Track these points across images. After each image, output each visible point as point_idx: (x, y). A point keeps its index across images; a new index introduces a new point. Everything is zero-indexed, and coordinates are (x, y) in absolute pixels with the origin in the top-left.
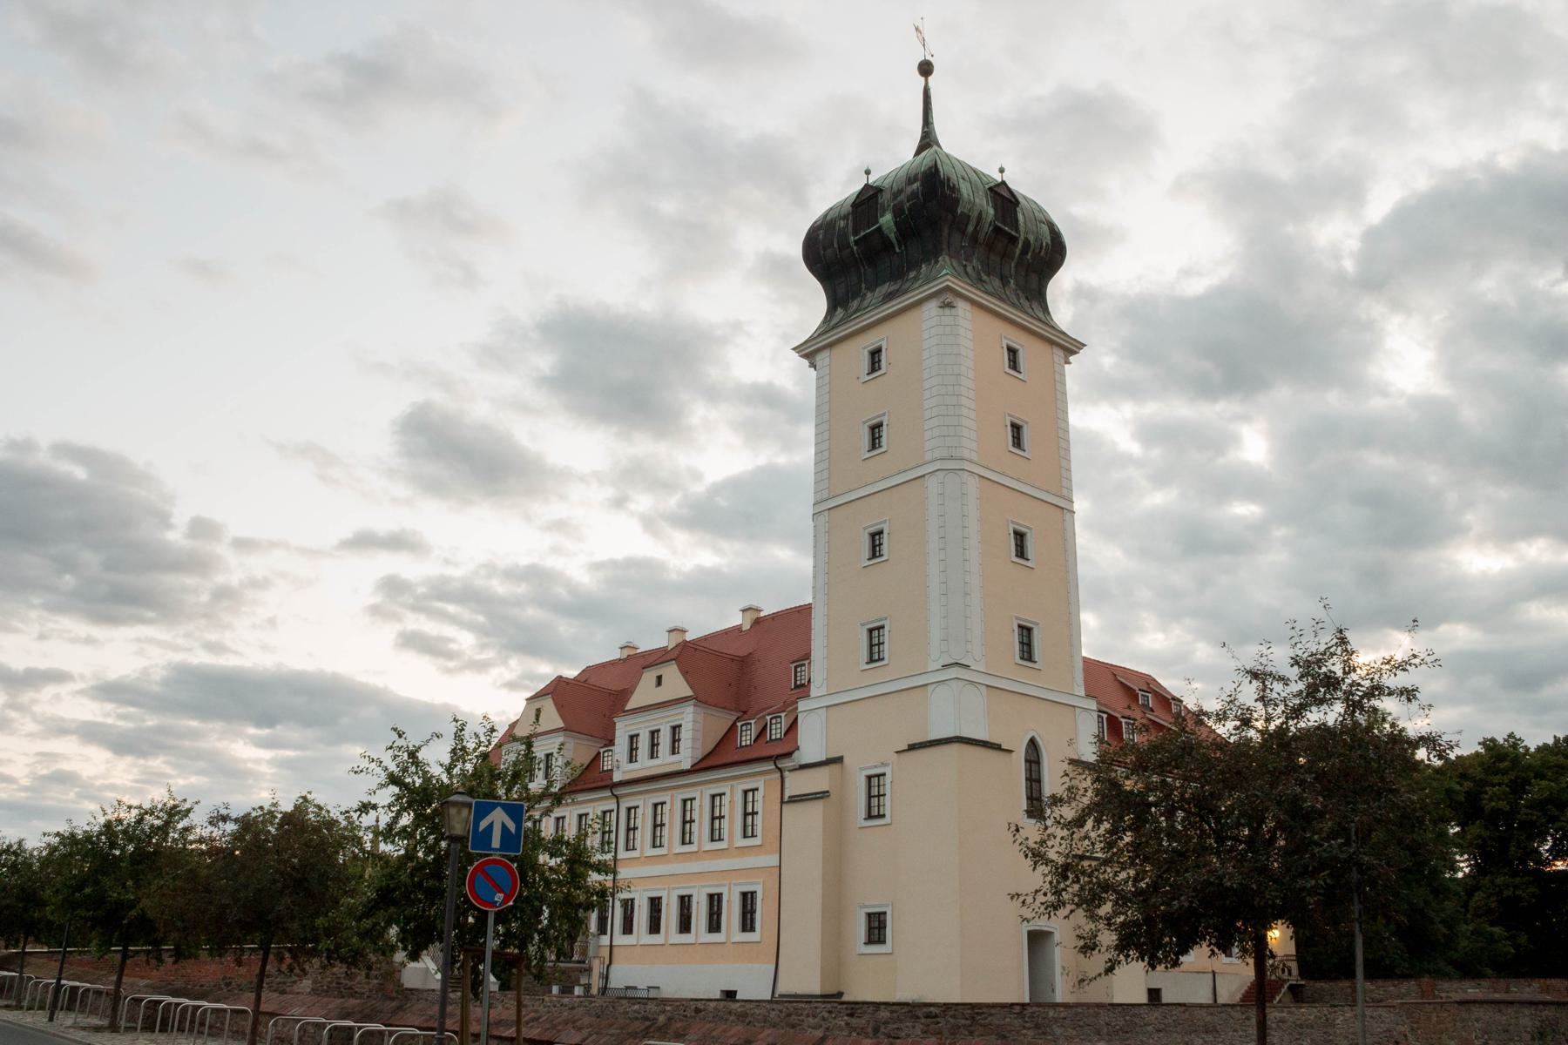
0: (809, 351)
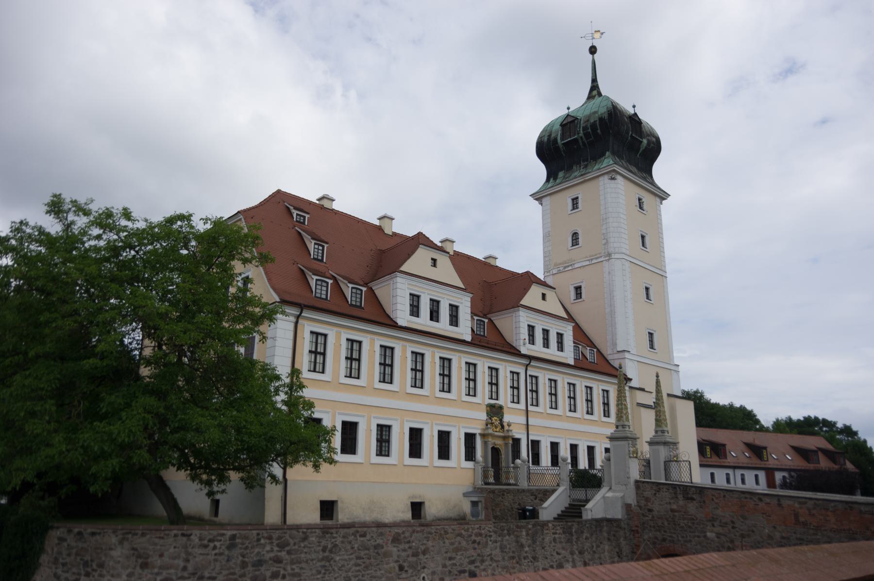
0: (538, 197)
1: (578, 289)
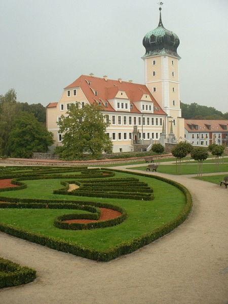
0: (143, 58)
1: (155, 89)
